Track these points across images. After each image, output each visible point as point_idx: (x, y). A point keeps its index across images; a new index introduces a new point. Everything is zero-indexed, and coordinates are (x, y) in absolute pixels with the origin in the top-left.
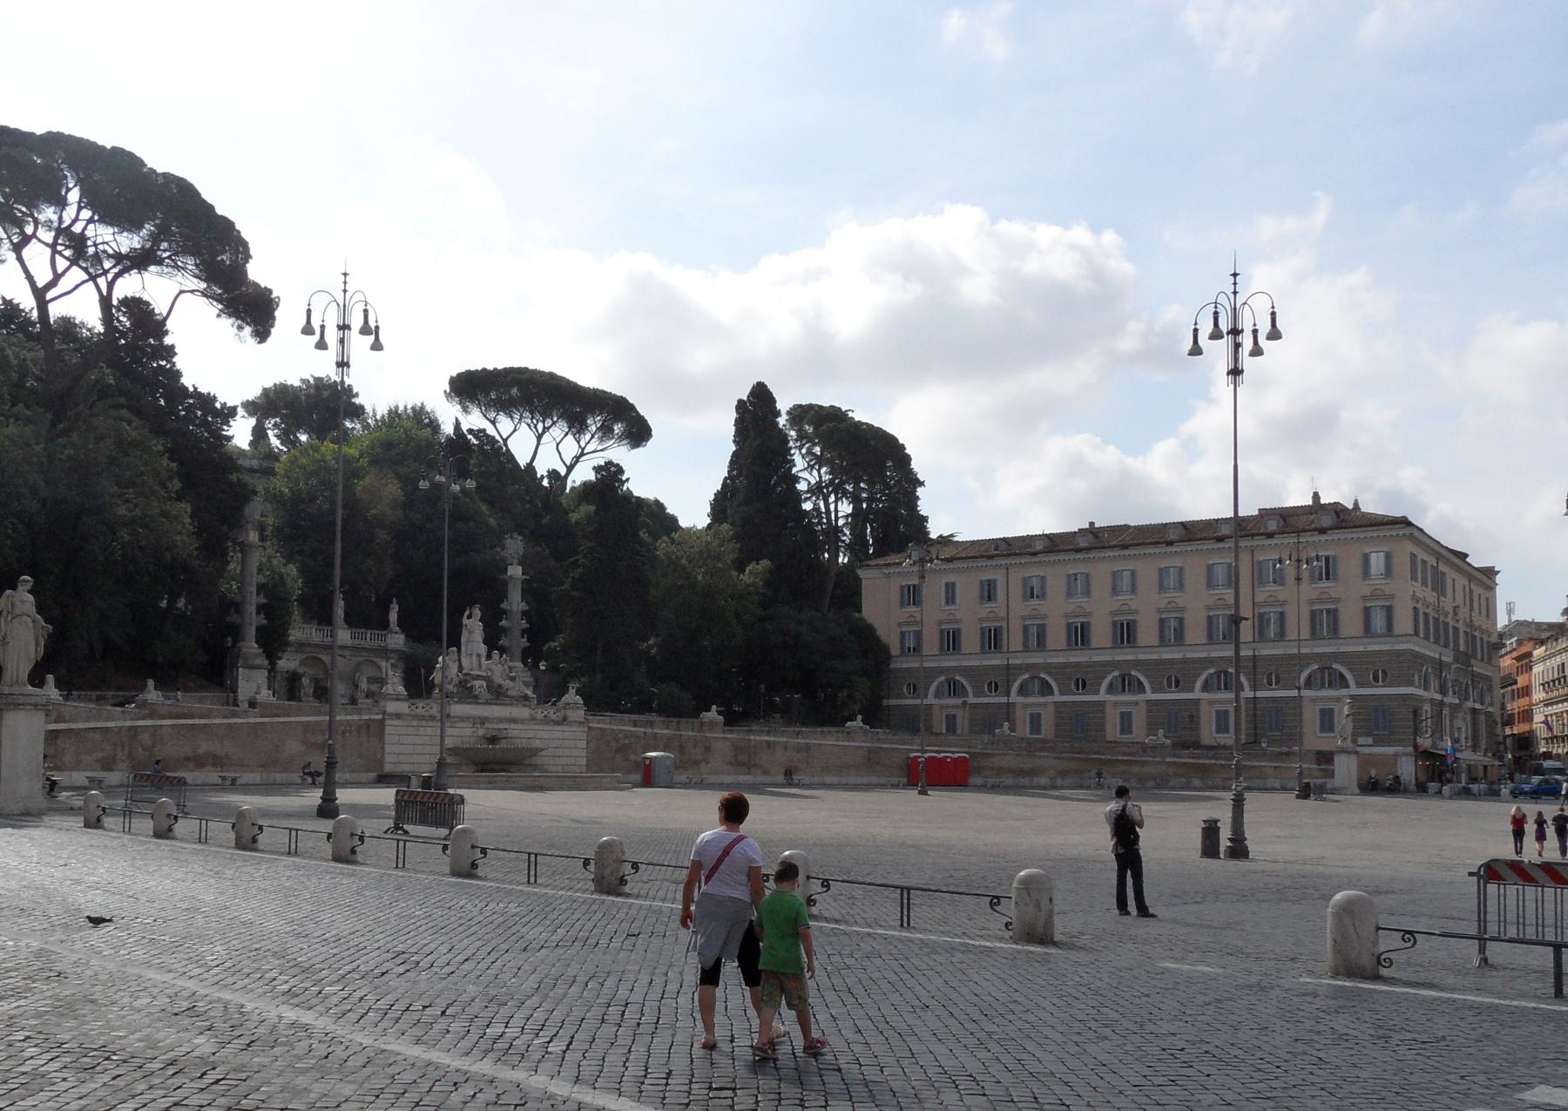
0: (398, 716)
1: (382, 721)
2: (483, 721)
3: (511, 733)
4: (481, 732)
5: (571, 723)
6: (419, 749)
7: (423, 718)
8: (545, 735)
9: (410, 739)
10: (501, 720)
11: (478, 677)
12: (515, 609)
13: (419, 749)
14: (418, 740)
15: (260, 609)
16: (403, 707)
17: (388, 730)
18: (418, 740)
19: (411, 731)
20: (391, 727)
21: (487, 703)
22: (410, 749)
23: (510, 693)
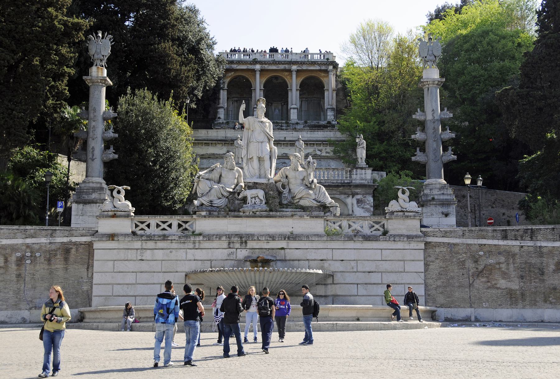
0: (112, 237)
1: (90, 245)
2: (244, 239)
3: (290, 254)
4: (242, 254)
5: (397, 237)
6: (143, 278)
7: (150, 238)
8: (352, 255)
9: (131, 266)
10: (272, 237)
11: (255, 186)
12: (429, 117)
13: (143, 278)
14: (144, 266)
15: (108, 144)
16: (124, 226)
17: (97, 255)
18: (144, 266)
19: (131, 255)
20: (102, 251)
21: (254, 215)
22: (130, 278)
23: (302, 203)
